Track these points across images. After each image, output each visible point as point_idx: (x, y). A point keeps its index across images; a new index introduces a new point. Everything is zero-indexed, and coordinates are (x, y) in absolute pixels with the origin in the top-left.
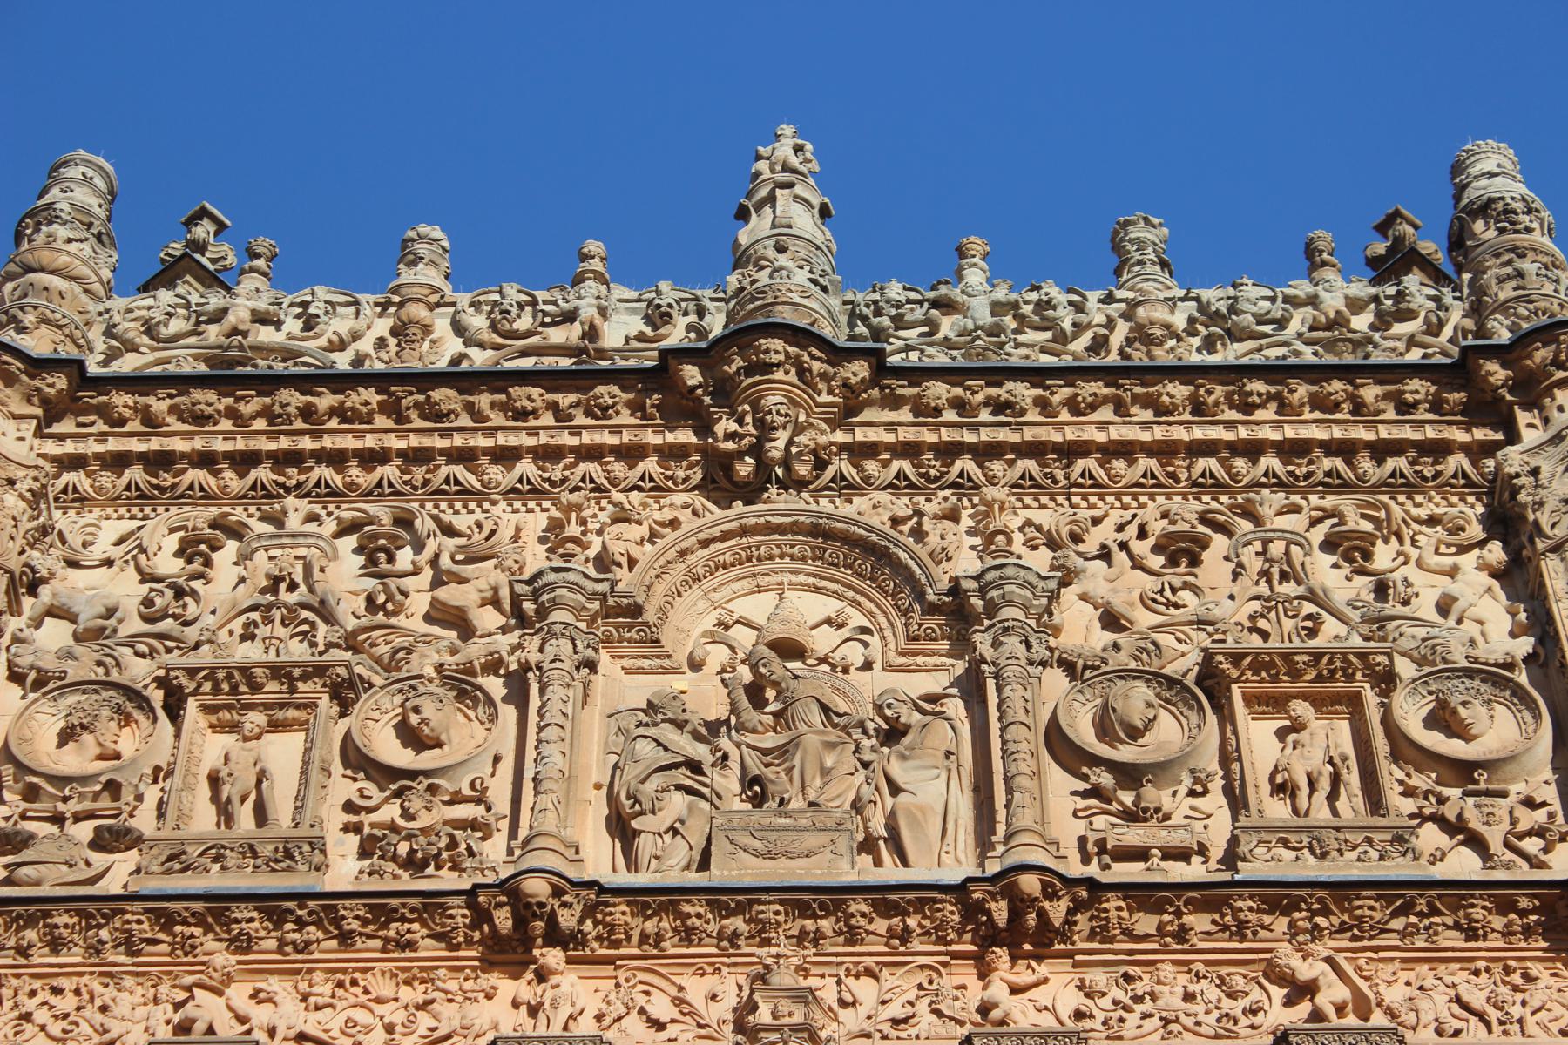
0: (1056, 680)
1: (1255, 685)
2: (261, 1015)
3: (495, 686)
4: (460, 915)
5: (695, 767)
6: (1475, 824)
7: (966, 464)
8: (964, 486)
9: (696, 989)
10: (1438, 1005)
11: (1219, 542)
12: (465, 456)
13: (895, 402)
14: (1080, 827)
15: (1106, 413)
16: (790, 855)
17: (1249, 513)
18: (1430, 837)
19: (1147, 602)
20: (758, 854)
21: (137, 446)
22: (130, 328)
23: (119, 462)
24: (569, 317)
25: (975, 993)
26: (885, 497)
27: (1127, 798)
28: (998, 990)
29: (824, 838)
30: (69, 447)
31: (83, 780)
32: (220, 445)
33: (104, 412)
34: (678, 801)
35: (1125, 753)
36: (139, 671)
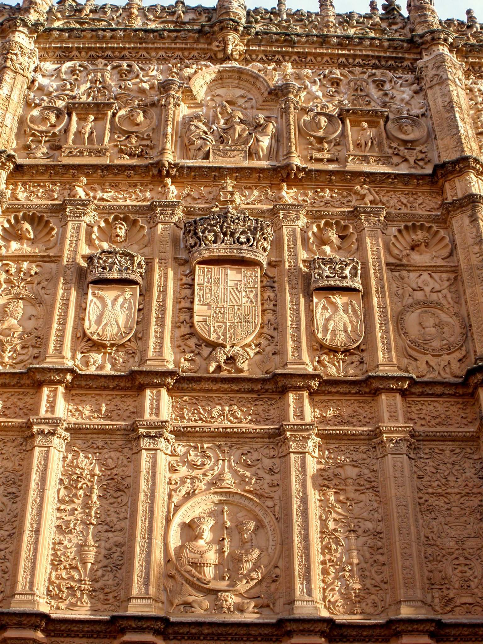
6: (407, 157)
8: (278, 63)
11: (345, 81)
12: (146, 49)
14: (305, 153)
16: (230, 157)
18: (395, 160)
20: (221, 156)
29: (239, 152)
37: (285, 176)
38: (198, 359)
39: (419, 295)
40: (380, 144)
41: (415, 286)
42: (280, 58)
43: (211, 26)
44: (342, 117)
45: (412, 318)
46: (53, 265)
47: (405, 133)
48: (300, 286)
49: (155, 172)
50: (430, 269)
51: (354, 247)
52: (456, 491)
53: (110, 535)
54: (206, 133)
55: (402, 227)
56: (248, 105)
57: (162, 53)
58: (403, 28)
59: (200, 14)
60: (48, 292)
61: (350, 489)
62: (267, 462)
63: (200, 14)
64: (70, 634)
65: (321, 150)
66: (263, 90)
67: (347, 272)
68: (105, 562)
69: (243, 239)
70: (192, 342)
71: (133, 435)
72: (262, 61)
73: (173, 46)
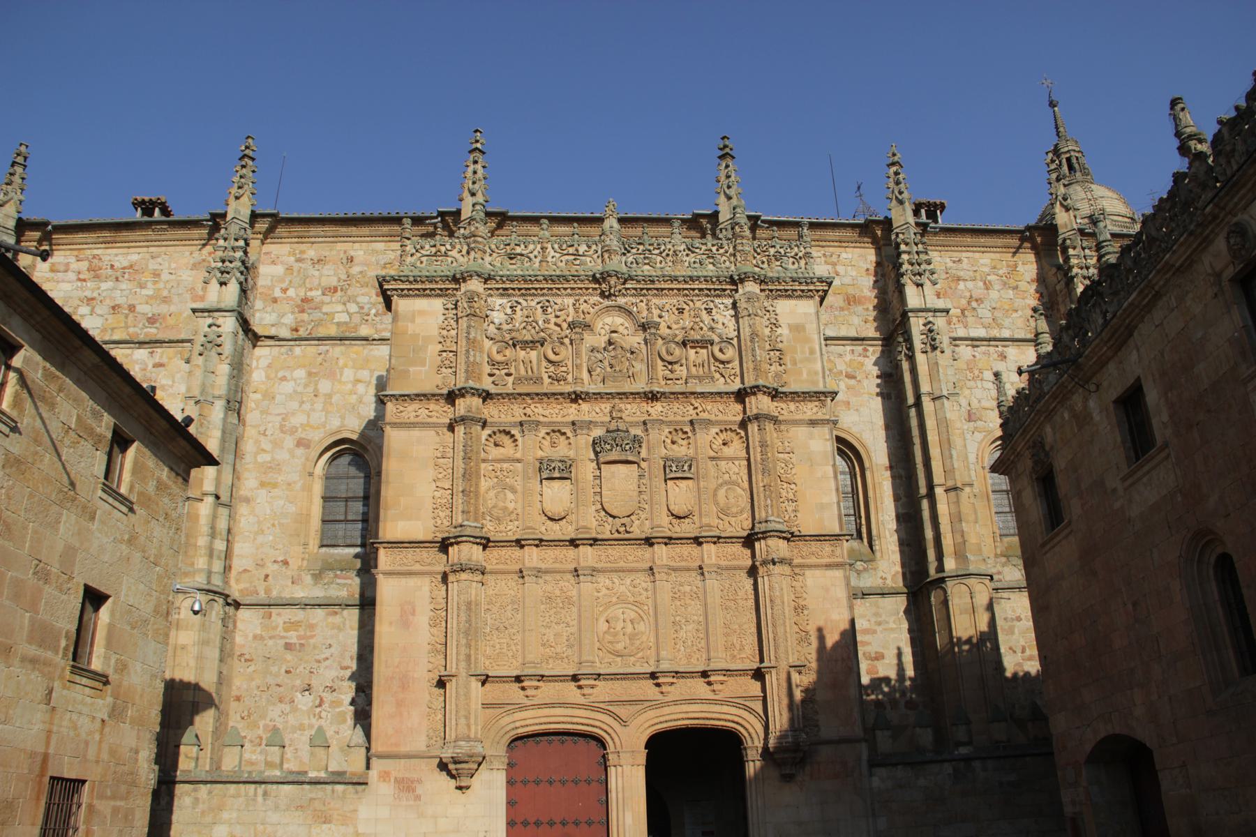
0: (660, 341)
1: (691, 345)
2: (536, 410)
3: (567, 341)
4: (567, 395)
5: (601, 361)
7: (645, 291)
8: (644, 295)
9: (603, 406)
10: (715, 410)
12: (558, 289)
13: (633, 280)
14: (662, 373)
15: (669, 282)
17: (692, 301)
18: (717, 375)
19: (675, 323)
21: (500, 286)
22: (493, 247)
23: (498, 289)
24: (573, 246)
25: (645, 408)
27: (670, 367)
28: (649, 409)
30: (489, 286)
32: (515, 286)
33: (495, 279)
34: (599, 369)
35: (669, 358)
36: (508, 337)
38: (606, 524)
41: (724, 470)
44: (684, 344)
45: (722, 492)
46: (519, 464)
47: (723, 353)
49: (573, 396)
50: (732, 459)
54: (601, 361)
55: (718, 430)
58: (727, 252)
60: (519, 483)
62: (644, 585)
64: (553, 681)
65: (671, 371)
67: (686, 468)
68: (567, 643)
69: (627, 447)
73: (576, 286)
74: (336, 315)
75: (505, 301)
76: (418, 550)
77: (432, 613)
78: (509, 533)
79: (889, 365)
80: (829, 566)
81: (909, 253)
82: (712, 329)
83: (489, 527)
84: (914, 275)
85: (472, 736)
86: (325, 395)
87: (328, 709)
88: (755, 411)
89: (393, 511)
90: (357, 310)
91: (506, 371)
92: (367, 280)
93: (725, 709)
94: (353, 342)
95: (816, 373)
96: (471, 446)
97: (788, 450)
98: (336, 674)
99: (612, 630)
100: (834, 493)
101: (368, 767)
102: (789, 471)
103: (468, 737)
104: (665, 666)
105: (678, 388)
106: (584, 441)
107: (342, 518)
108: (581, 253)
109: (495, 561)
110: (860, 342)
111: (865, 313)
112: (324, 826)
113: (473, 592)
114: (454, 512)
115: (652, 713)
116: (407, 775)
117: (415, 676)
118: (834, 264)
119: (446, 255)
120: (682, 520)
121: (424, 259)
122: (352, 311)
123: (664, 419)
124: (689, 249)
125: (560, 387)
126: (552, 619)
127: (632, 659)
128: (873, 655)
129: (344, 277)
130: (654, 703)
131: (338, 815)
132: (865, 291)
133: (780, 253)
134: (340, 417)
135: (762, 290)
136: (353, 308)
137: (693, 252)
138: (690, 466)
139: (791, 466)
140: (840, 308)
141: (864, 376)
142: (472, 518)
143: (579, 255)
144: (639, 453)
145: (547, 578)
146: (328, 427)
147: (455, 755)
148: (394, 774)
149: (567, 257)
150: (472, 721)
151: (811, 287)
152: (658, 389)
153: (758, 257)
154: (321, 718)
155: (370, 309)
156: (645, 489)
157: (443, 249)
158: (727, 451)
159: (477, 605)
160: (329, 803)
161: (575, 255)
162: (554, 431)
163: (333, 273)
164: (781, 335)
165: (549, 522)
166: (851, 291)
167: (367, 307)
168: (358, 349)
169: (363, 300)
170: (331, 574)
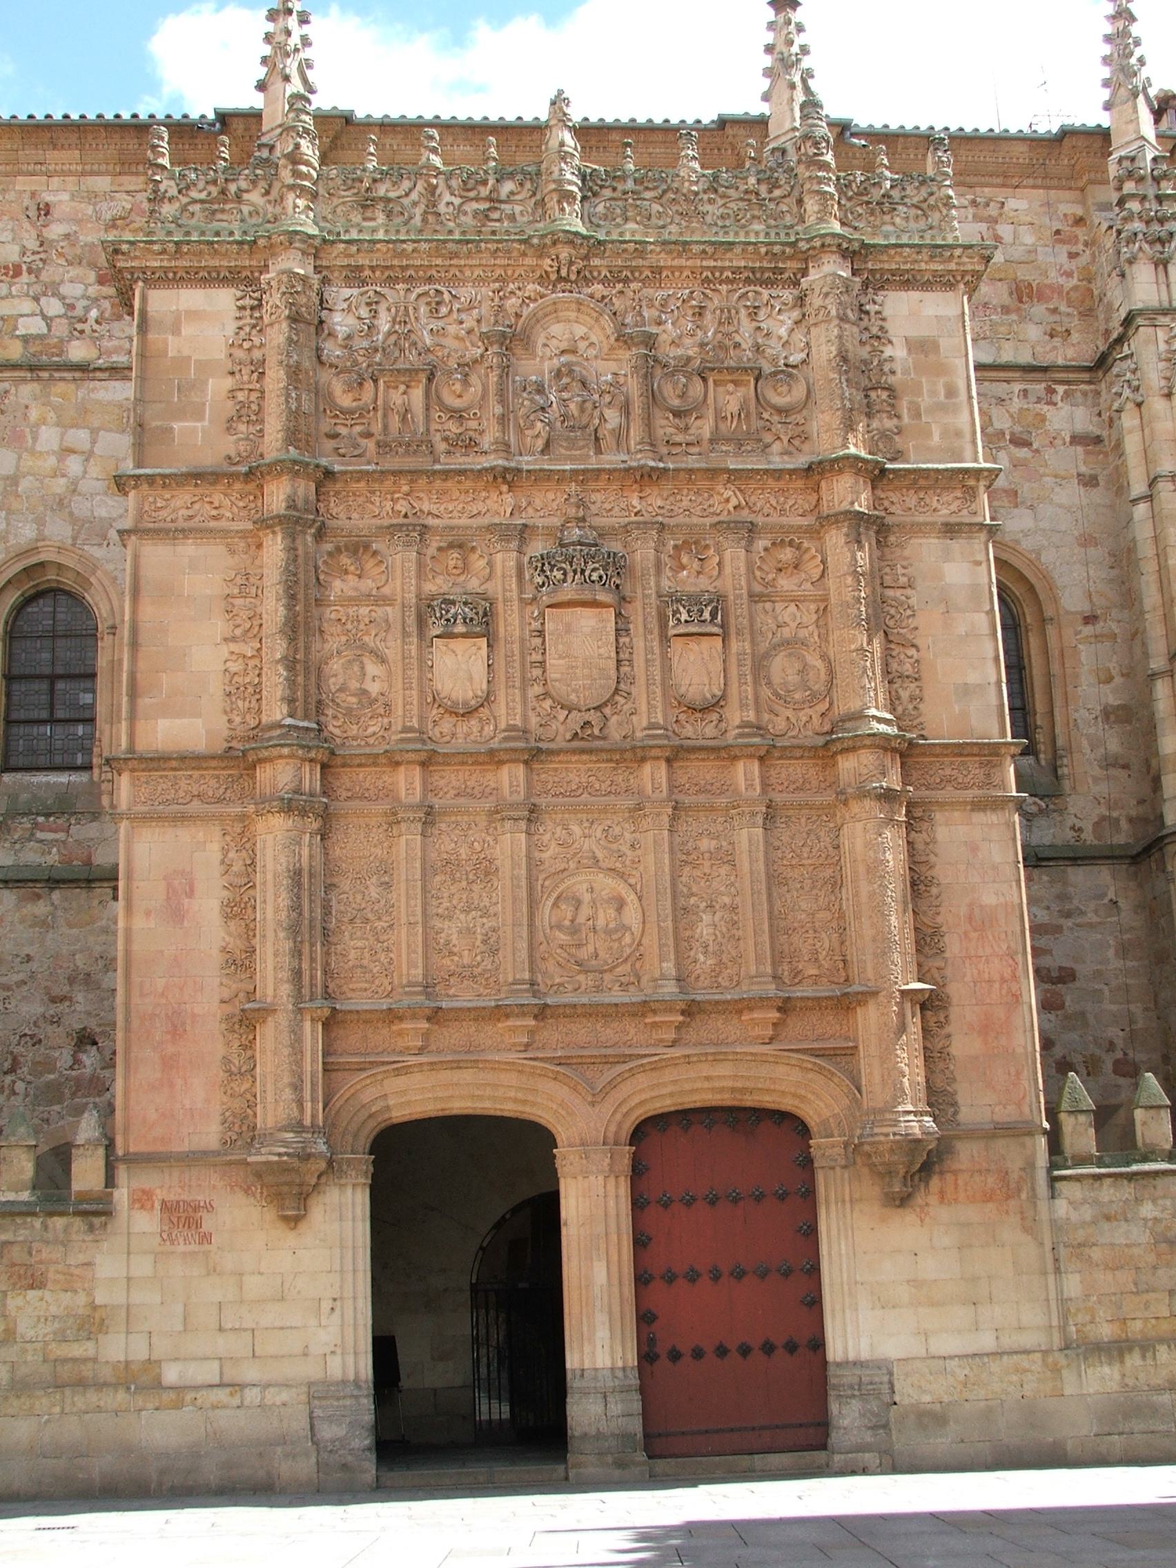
5: (543, 409)
8: (626, 281)
11: (711, 306)
26: (600, 287)
28: (635, 502)
31: (352, 412)
34: (539, 424)
35: (676, 402)
37: (638, 478)
39: (786, 632)
40: (748, 415)
42: (629, 274)
43: (543, 237)
47: (779, 394)
48: (656, 631)
50: (797, 601)
51: (715, 573)
52: (810, 861)
53: (485, 920)
54: (543, 409)
55: (768, 543)
56: (592, 352)
57: (478, 272)
59: (521, 185)
60: (389, 644)
61: (707, 863)
63: (521, 185)
66: (609, 332)
67: (707, 615)
68: (483, 948)
69: (595, 577)
70: (547, 704)
71: (498, 816)
72: (604, 281)
74: (21, 320)
75: (355, 291)
76: (196, 774)
77: (226, 893)
78: (371, 741)
79: (1096, 419)
80: (979, 806)
81: (1144, 198)
82: (758, 349)
83: (331, 728)
84: (1151, 243)
85: (307, 1121)
86: (7, 478)
87: (29, 1078)
88: (838, 509)
89: (147, 700)
90: (63, 311)
91: (358, 429)
92: (79, 251)
93: (781, 1070)
94: (57, 375)
95: (958, 434)
96: (295, 575)
97: (903, 580)
98: (42, 1010)
99: (567, 923)
100: (990, 665)
101: (110, 1181)
102: (904, 624)
103: (300, 1123)
104: (670, 989)
105: (692, 462)
106: (506, 560)
107: (44, 715)
108: (503, 196)
109: (345, 794)
110: (1039, 375)
111: (1052, 319)
112: (31, 1294)
113: (305, 852)
114: (264, 702)
115: (642, 1080)
116: (185, 1197)
117: (198, 1010)
118: (993, 221)
119: (238, 197)
120: (699, 715)
121: (196, 208)
122: (50, 314)
123: (666, 521)
124: (716, 191)
125: (467, 459)
126: (455, 902)
127: (607, 977)
128: (1055, 974)
129: (32, 244)
130: (645, 1061)
131: (58, 1272)
132: (1053, 274)
133: (890, 197)
134: (34, 521)
135: (855, 272)
136: (54, 307)
137: (723, 196)
138: (714, 615)
139: (909, 612)
140: (1003, 307)
141: (1047, 442)
142: (300, 712)
143: (501, 202)
144: (617, 586)
145: (443, 826)
146: (12, 542)
147: (276, 1158)
148: (160, 1195)
149: (475, 205)
150: (307, 1095)
151: (953, 266)
152: (652, 464)
153: (849, 205)
154: (14, 1093)
155: (87, 309)
156: (627, 656)
157: (233, 188)
158: (786, 583)
159: (311, 875)
160: (39, 1251)
161: (489, 199)
162: (451, 546)
163: (10, 238)
164: (891, 359)
165: (447, 725)
166: (1024, 274)
167: (81, 304)
168: (64, 391)
169: (72, 290)
170: (26, 823)
